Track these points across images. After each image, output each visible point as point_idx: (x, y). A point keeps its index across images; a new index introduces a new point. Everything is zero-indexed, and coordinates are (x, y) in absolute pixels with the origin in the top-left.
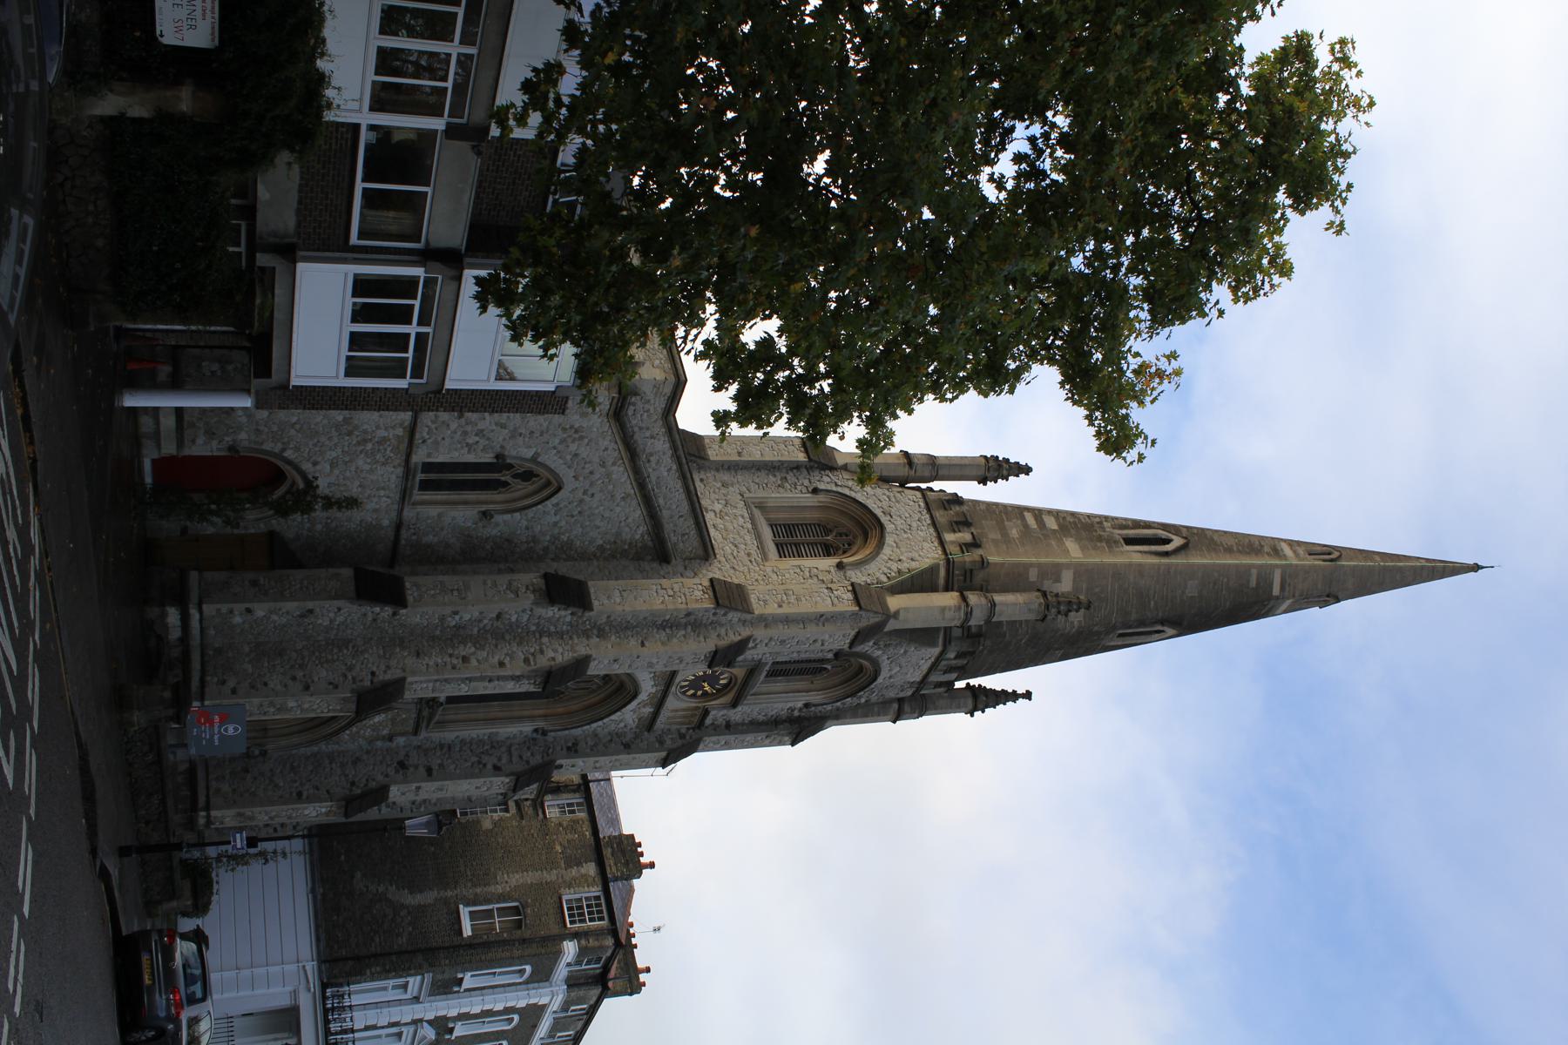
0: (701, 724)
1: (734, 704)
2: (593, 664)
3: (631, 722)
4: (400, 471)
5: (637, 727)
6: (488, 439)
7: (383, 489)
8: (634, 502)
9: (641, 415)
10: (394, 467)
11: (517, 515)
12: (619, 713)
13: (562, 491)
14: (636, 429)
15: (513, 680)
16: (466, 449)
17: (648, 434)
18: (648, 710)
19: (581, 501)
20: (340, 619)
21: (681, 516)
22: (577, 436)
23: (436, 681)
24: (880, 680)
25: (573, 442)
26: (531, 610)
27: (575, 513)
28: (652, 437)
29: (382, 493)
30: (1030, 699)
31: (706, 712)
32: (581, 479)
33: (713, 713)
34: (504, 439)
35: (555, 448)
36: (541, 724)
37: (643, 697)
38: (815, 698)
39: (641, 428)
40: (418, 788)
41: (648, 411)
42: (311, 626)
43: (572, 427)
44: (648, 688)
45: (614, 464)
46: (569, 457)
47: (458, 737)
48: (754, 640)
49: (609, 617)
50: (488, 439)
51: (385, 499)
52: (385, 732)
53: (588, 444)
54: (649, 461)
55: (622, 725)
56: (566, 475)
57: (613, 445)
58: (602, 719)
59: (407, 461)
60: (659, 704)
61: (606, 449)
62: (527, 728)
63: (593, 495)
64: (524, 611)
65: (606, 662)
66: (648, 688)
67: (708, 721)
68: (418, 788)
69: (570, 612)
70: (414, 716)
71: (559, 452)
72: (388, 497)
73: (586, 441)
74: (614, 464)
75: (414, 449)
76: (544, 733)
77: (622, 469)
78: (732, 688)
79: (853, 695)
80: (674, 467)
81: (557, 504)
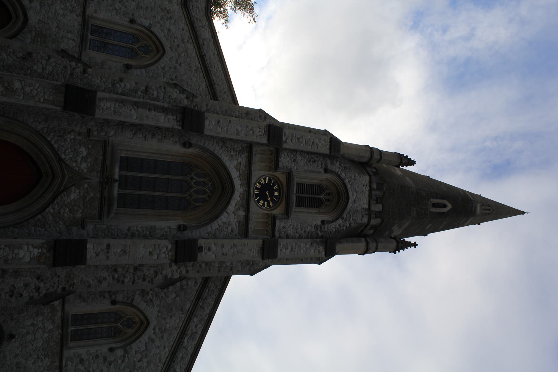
0: (273, 235)
1: (287, 213)
2: (207, 123)
3: (234, 226)
4: (80, 19)
5: (239, 233)
6: (126, 7)
7: (71, 32)
8: (201, 74)
9: (196, 10)
10: (77, 16)
11: (143, 70)
12: (225, 214)
13: (164, 57)
14: (195, 19)
15: (163, 112)
16: (115, 11)
17: (200, 25)
18: (242, 213)
19: (175, 68)
20: (50, 68)
21: (225, 93)
22: (168, 16)
23: (116, 100)
24: (350, 205)
25: (167, 20)
26: (164, 88)
27: (174, 77)
28: (203, 27)
29: (70, 36)
30: (415, 247)
31: (274, 218)
32: (174, 49)
33: (278, 222)
34: (134, 9)
35: (159, 23)
36: (182, 223)
37: (237, 197)
38: (326, 218)
39: (197, 19)
40: (108, 246)
41: (198, 8)
42: (29, 71)
43: (165, 9)
44: (239, 189)
45: (188, 42)
46: (166, 31)
47: (129, 230)
48: (285, 134)
49: (207, 105)
50: (126, 7)
51: (71, 41)
52: (79, 215)
53: (174, 24)
54: (204, 44)
55: (230, 230)
56: (167, 45)
57: (186, 28)
58: (217, 217)
59: (84, 12)
60: (247, 209)
61: (183, 30)
62: (173, 224)
63: (181, 64)
64: (160, 87)
65: (214, 123)
66: (239, 189)
67: (277, 234)
68: (108, 246)
69: (185, 96)
70: (98, 196)
71: (161, 26)
72: (73, 40)
73: (173, 20)
74: (188, 42)
75: (88, 4)
76: (185, 228)
77: (192, 47)
78: (282, 200)
79: (340, 216)
80: (216, 53)
81: (163, 68)
